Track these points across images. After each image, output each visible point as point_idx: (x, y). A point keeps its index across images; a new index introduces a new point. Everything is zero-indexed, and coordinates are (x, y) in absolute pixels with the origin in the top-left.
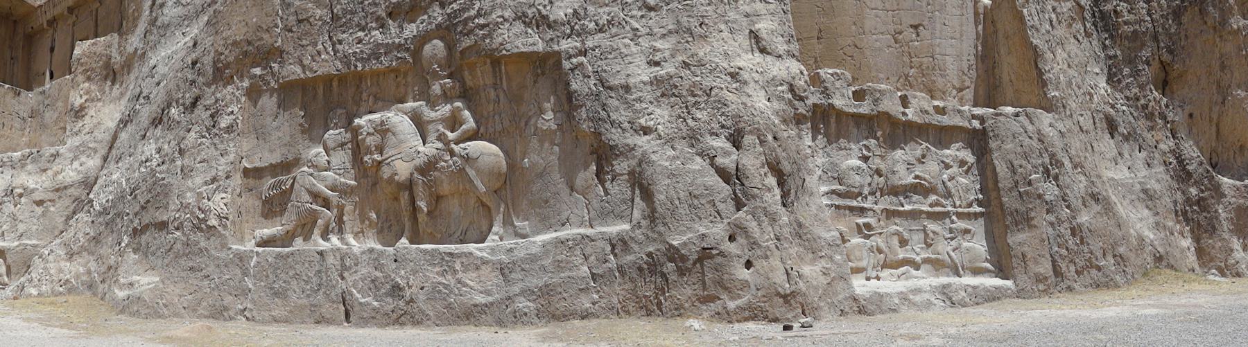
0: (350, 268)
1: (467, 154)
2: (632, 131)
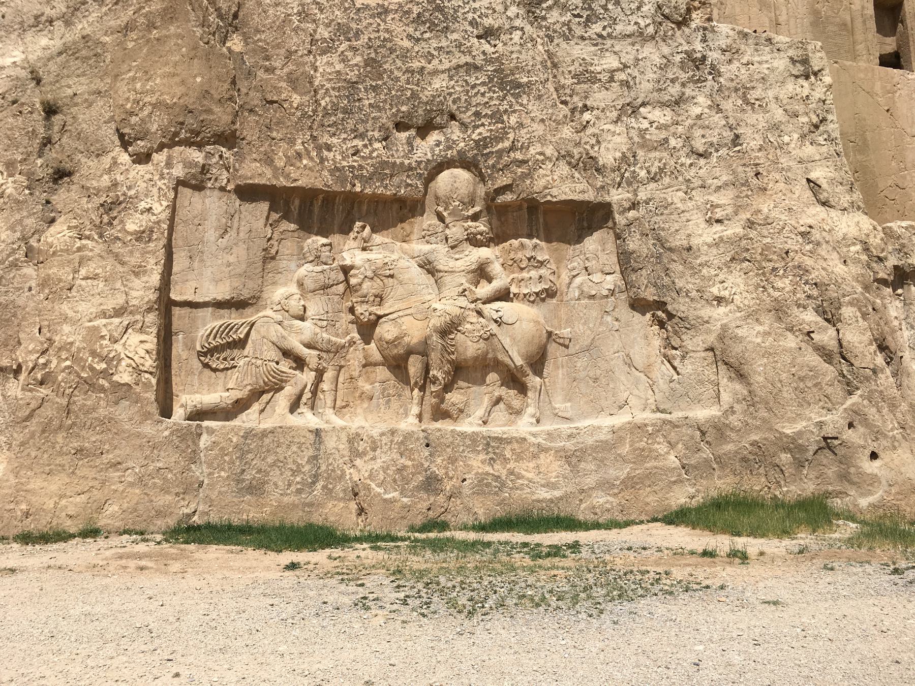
0: (364, 453)
2: (704, 302)
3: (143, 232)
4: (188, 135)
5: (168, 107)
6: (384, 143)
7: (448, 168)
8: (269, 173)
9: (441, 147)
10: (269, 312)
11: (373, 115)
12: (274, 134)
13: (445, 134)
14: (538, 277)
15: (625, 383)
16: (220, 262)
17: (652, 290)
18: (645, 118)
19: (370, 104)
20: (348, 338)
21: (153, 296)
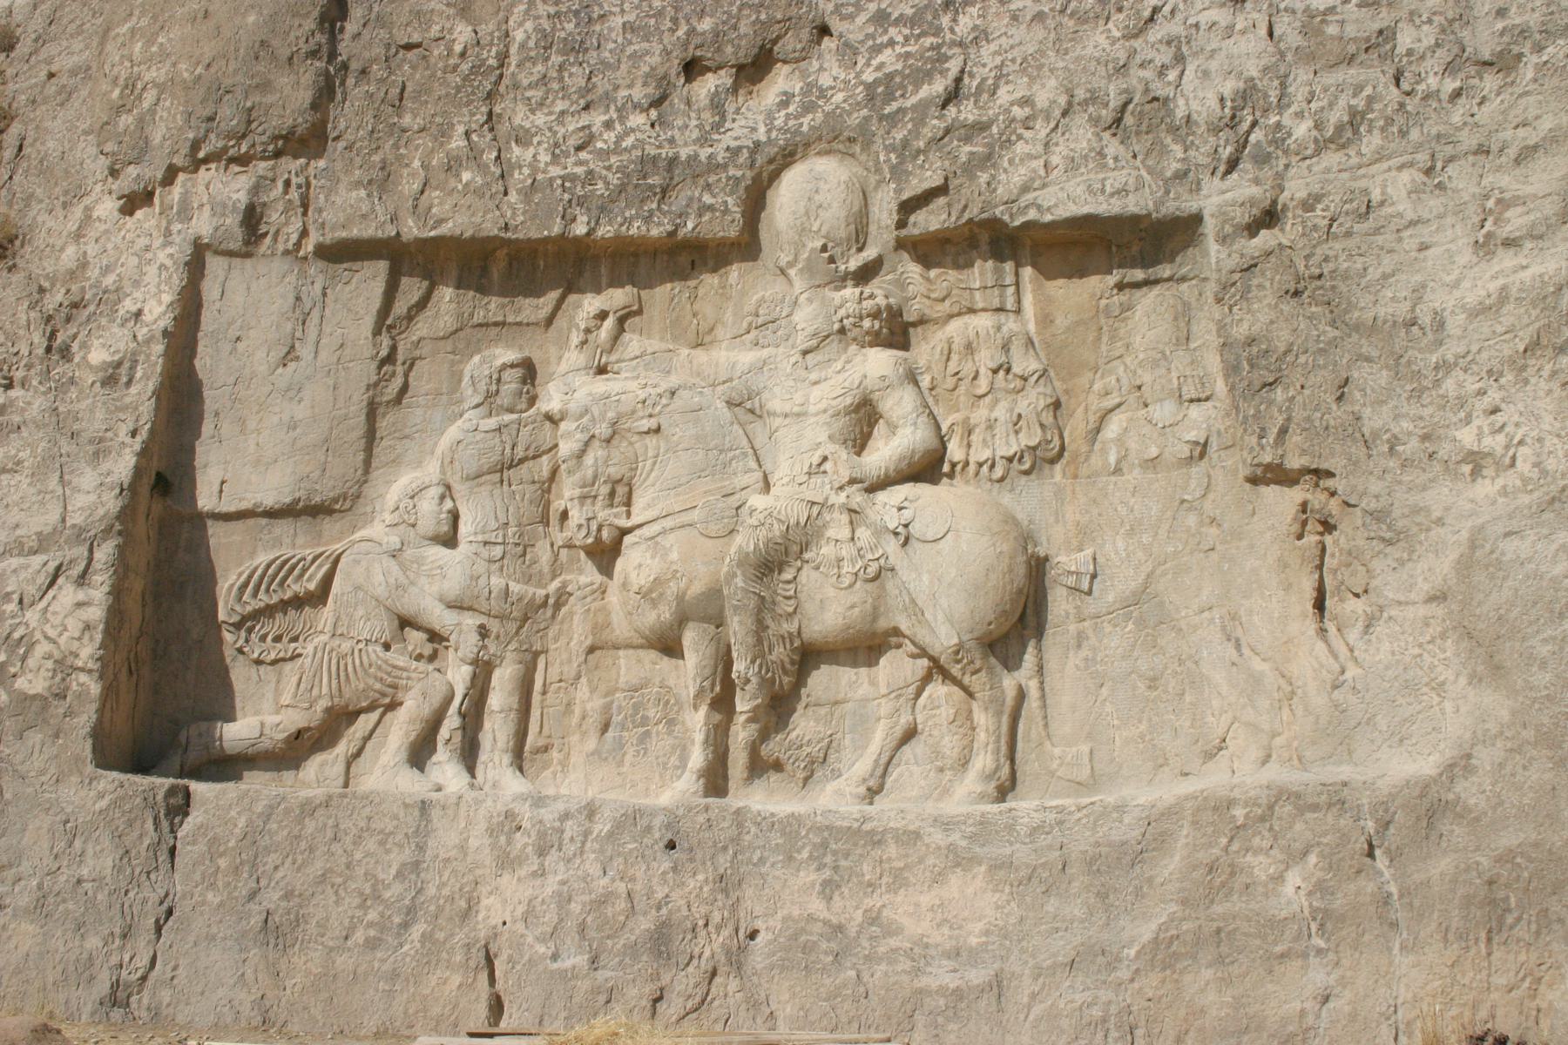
0: (520, 860)
3: (119, 364)
6: (654, 113)
9: (791, 109)
10: (376, 530)
11: (629, 50)
12: (407, 120)
13: (804, 75)
15: (1224, 689)
20: (555, 584)
21: (111, 504)
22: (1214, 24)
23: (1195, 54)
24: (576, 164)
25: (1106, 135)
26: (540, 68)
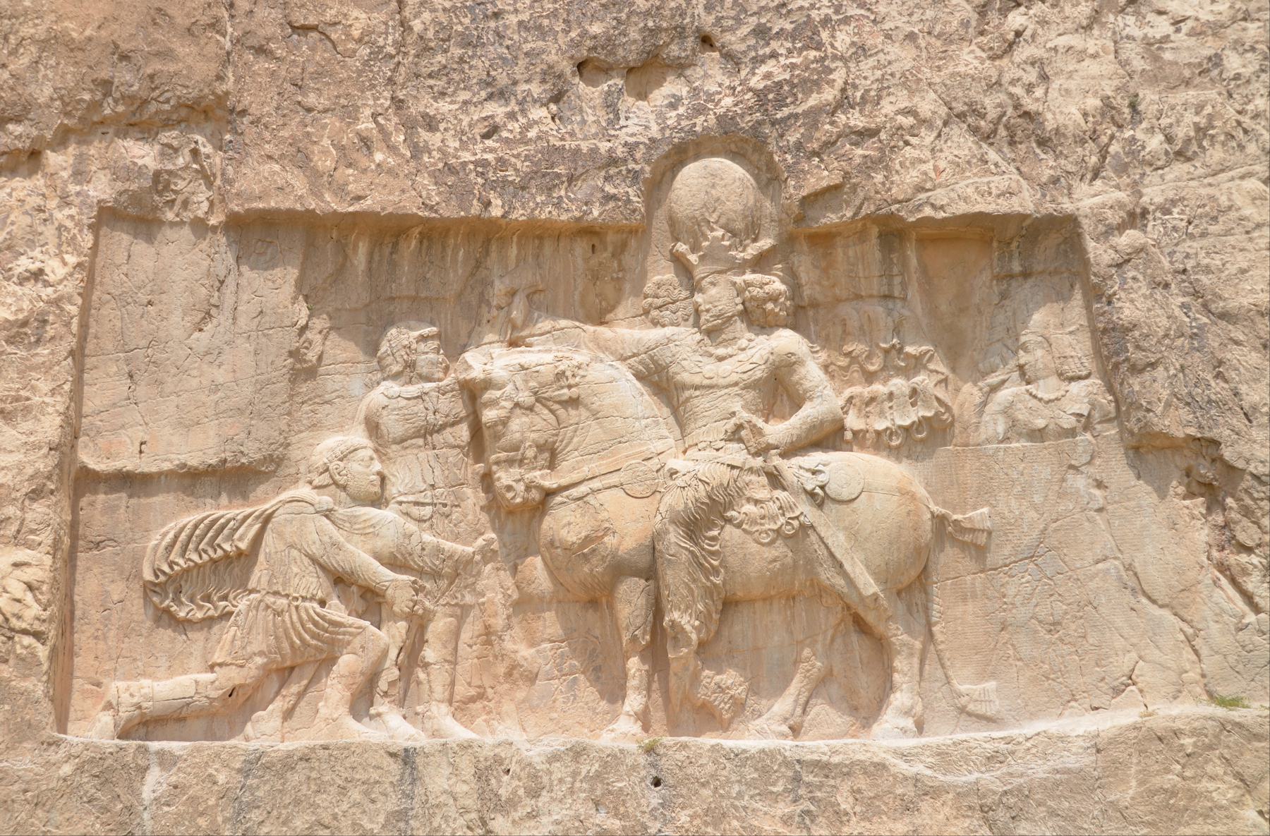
0: (512, 803)
1: (822, 488)
3: (25, 323)
4: (121, 109)
5: (73, 48)
6: (553, 107)
7: (697, 157)
8: (299, 184)
9: (681, 110)
10: (303, 491)
11: (527, 47)
12: (311, 99)
14: (907, 391)
16: (194, 383)
17: (1184, 413)
18: (1160, 13)
19: (520, 23)
20: (480, 542)
21: (43, 463)
22: (1070, 48)
23: (1056, 74)
24: (484, 151)
25: (985, 146)
26: (440, 58)
